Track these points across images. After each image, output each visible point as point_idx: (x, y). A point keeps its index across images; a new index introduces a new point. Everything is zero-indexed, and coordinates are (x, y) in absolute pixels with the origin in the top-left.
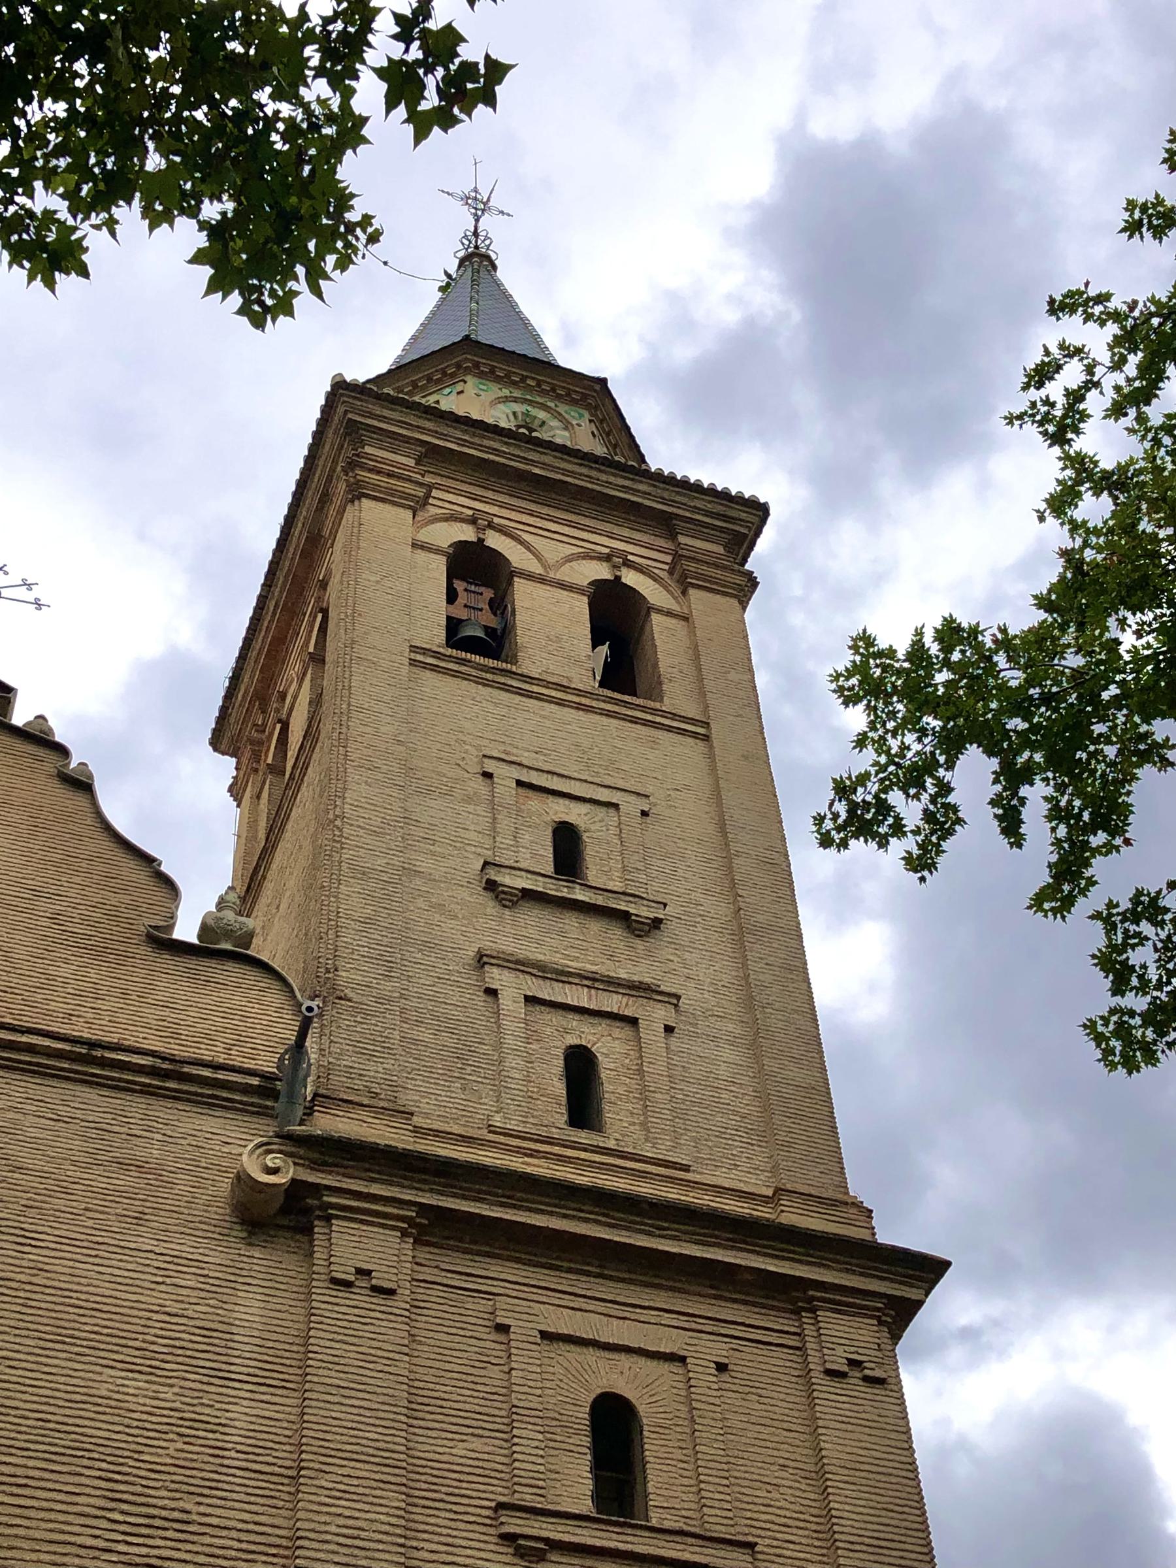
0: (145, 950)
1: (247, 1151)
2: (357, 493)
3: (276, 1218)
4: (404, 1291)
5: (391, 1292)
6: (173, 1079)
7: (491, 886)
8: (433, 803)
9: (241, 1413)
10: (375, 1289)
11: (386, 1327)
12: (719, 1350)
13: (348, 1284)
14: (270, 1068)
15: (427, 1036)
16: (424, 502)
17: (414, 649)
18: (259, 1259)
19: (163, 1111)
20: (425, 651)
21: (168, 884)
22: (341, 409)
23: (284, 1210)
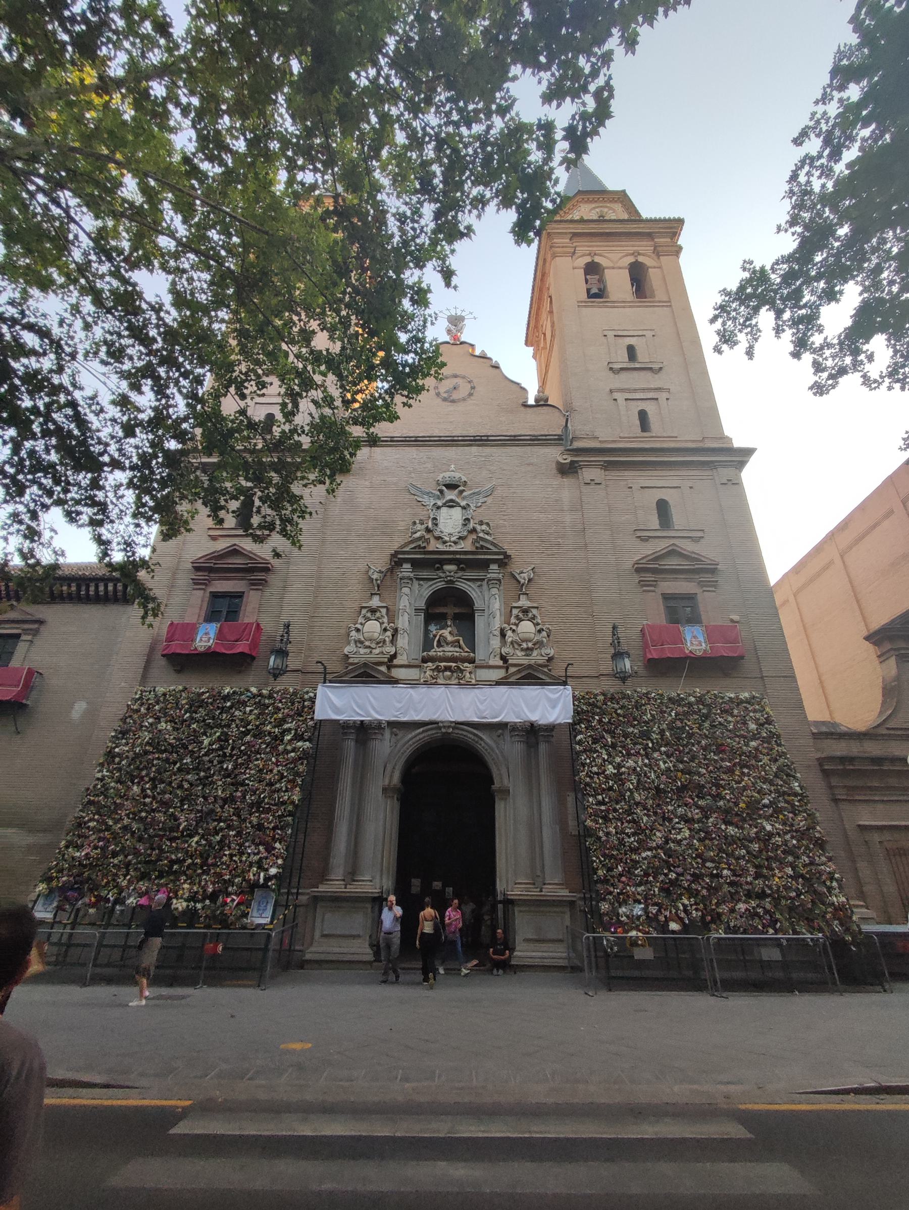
2: (554, 256)
3: (567, 470)
6: (537, 440)
7: (611, 369)
9: (568, 518)
12: (690, 484)
14: (560, 432)
16: (574, 253)
18: (566, 481)
19: (536, 449)
21: (524, 389)
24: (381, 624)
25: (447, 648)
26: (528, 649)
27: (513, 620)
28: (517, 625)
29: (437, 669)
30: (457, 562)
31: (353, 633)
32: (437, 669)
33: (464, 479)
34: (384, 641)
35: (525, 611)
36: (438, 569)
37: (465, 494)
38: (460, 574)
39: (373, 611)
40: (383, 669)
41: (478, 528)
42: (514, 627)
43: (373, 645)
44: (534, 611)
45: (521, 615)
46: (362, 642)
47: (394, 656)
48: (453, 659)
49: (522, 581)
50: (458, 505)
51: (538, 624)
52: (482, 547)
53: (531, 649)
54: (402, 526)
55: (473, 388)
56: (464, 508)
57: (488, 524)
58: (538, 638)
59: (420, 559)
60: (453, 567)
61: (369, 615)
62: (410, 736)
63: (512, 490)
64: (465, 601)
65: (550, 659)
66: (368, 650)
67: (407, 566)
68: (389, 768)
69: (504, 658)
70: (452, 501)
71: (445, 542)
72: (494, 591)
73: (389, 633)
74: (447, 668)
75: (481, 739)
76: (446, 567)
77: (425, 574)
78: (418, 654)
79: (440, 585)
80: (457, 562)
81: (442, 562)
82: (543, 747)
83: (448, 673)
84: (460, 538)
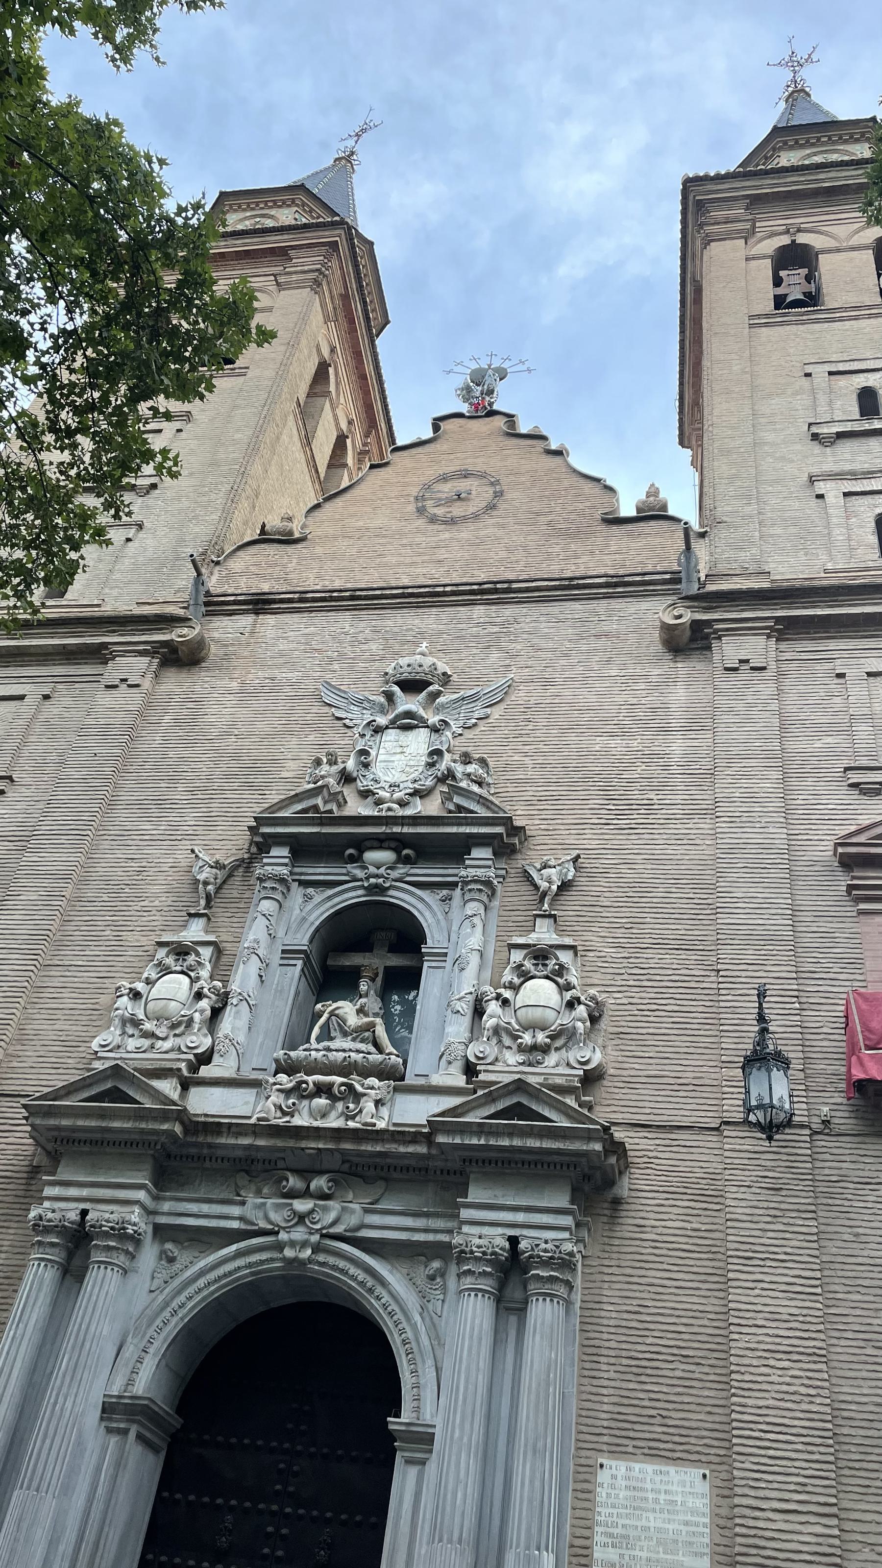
0: (603, 527)
1: (659, 611)
2: (707, 243)
3: (688, 642)
4: (772, 666)
5: (764, 668)
6: (619, 586)
8: (773, 402)
10: (752, 668)
11: (766, 688)
13: (735, 669)
14: (676, 568)
15: (779, 531)
16: (753, 231)
17: (751, 317)
18: (683, 667)
20: (759, 316)
21: (610, 489)
22: (691, 198)
23: (692, 640)
24: (193, 981)
25: (339, 1043)
26: (534, 1048)
27: (508, 976)
28: (515, 988)
29: (298, 1091)
30: (396, 843)
31: (124, 1001)
32: (298, 1091)
33: (442, 667)
34: (190, 1021)
35: (540, 955)
36: (352, 859)
37: (441, 700)
38: (401, 870)
39: (181, 951)
40: (168, 1087)
41: (459, 769)
42: (507, 994)
43: (161, 1032)
44: (565, 957)
45: (528, 965)
46: (135, 1023)
47: (206, 1058)
48: (345, 1069)
49: (544, 885)
50: (423, 723)
51: (568, 987)
52: (460, 808)
53: (545, 1050)
54: (290, 770)
55: (499, 494)
56: (435, 730)
57: (483, 762)
58: (565, 1019)
59: (314, 839)
60: (386, 856)
61: (170, 961)
62: (202, 1264)
63: (553, 690)
64: (408, 937)
65: (592, 1078)
66: (146, 1043)
67: (281, 852)
68: (130, 1352)
69: (470, 1070)
70: (409, 714)
71: (379, 802)
72: (473, 907)
73: (204, 1004)
74: (322, 1090)
76: (371, 856)
77: (319, 872)
78: (264, 1052)
79: (354, 896)
80: (396, 843)
81: (362, 844)
82: (542, 1313)
83: (322, 1102)
84: (416, 793)
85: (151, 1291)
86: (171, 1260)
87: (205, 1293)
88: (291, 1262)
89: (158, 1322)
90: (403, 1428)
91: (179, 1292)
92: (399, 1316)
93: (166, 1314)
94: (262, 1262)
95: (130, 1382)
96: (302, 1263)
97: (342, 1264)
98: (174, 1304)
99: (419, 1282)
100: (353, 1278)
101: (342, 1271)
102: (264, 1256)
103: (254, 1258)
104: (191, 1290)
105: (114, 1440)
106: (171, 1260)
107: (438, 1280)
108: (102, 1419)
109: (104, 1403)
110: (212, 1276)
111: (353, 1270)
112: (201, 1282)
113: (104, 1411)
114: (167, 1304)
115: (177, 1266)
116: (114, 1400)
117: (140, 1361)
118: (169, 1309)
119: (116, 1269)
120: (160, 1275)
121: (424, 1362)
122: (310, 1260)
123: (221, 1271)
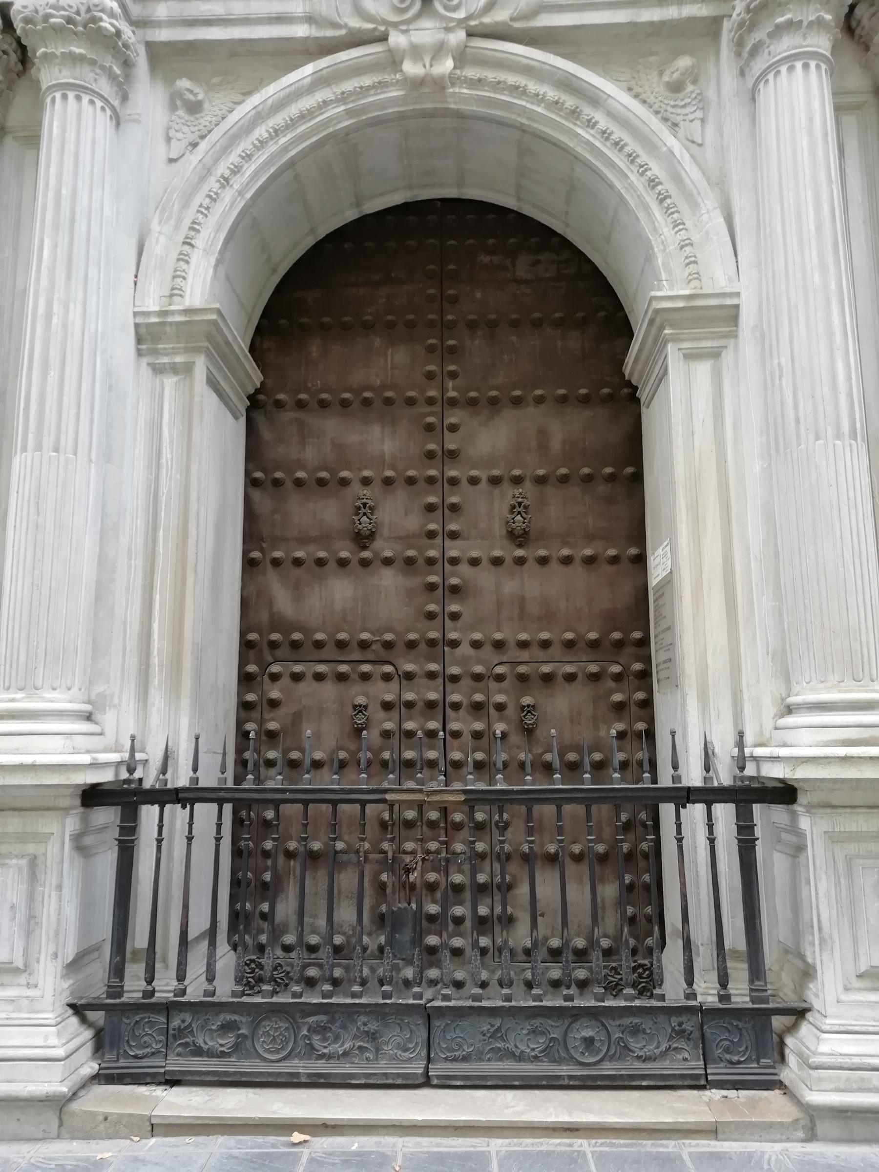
68: (162, 246)
75: (594, 98)
85: (171, 161)
86: (194, 108)
87: (273, 148)
88: (417, 84)
89: (200, 198)
90: (680, 304)
91: (226, 149)
92: (632, 146)
93: (212, 183)
94: (364, 91)
95: (175, 293)
96: (439, 84)
97: (512, 79)
98: (222, 168)
99: (651, 99)
100: (538, 98)
101: (515, 90)
102: (367, 81)
103: (349, 86)
104: (245, 145)
105: (170, 382)
106: (194, 108)
107: (690, 88)
108: (140, 353)
109: (137, 326)
110: (279, 119)
111: (533, 87)
112: (261, 131)
113: (139, 340)
114: (207, 172)
115: (206, 119)
116: (154, 320)
117: (184, 258)
118: (213, 179)
119: (99, 103)
120: (179, 135)
121: (694, 206)
122: (453, 80)
123: (294, 110)
